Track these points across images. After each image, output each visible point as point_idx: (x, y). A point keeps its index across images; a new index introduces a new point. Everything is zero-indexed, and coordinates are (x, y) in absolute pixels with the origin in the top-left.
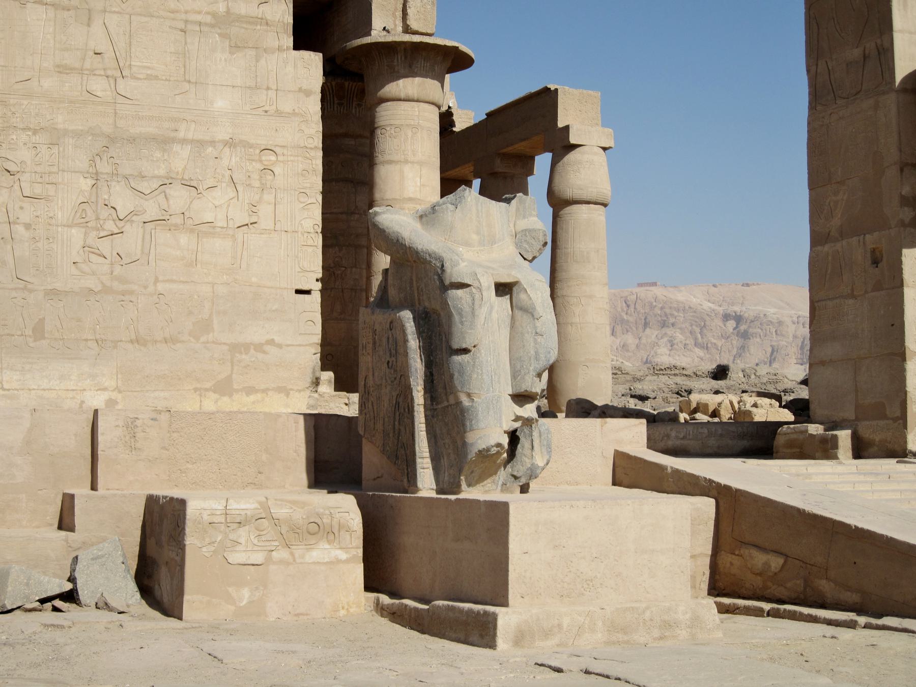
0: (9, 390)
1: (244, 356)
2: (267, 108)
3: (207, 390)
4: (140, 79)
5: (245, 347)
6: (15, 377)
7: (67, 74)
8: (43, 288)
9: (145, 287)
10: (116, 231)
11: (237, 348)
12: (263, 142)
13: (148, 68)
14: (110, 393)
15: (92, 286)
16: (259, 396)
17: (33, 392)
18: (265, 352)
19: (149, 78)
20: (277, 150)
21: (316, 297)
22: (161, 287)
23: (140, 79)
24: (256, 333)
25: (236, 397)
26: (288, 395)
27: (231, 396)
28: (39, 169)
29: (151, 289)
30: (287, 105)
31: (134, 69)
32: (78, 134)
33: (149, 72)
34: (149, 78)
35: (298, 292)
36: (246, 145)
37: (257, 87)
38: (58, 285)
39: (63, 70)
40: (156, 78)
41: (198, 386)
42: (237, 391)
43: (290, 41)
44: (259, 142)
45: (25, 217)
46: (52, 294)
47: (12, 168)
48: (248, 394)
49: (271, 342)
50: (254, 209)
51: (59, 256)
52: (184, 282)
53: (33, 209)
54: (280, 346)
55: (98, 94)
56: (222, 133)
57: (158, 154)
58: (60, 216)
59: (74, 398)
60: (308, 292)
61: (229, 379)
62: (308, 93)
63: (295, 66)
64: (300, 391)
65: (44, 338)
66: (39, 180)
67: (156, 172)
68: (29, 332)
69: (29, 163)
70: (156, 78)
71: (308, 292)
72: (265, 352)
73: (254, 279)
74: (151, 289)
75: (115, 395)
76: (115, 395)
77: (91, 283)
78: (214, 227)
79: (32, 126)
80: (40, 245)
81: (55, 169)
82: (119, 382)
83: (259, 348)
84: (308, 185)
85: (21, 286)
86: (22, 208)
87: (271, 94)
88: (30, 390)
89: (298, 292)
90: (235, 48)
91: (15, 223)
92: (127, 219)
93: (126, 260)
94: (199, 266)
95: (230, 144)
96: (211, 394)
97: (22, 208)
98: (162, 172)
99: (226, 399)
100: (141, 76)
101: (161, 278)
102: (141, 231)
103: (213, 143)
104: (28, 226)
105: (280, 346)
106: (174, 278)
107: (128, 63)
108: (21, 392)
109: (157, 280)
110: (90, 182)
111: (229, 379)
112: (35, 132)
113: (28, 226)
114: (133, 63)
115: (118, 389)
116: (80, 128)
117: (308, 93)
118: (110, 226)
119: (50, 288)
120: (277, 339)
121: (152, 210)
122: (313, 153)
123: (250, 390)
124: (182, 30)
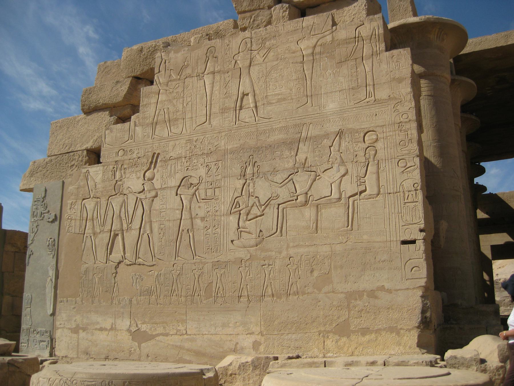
0: (190, 335)
1: (358, 302)
2: (367, 100)
3: (328, 332)
4: (274, 103)
5: (359, 294)
6: (194, 326)
7: (226, 112)
8: (212, 261)
9: (280, 253)
10: (259, 214)
11: (352, 296)
12: (366, 126)
13: (279, 94)
14: (257, 337)
15: (243, 256)
16: (373, 336)
17: (205, 336)
18: (376, 297)
19: (279, 101)
20: (378, 129)
21: (420, 245)
22: (292, 252)
23: (274, 103)
24: (366, 283)
25: (353, 337)
26: (398, 333)
27: (348, 337)
28: (210, 179)
29: (284, 253)
30: (382, 94)
31: (270, 98)
32: (232, 152)
33: (279, 97)
34: (279, 101)
35: (404, 242)
36: (352, 132)
37: (358, 87)
38: (222, 258)
39: (224, 110)
40: (284, 99)
41: (322, 329)
42: (354, 332)
43: (383, 46)
44: (363, 127)
45: (202, 214)
46: (217, 265)
47: (195, 181)
48: (363, 334)
49: (382, 288)
50: (362, 180)
51: (222, 237)
52: (308, 246)
53: (206, 207)
54: (389, 291)
55: (247, 120)
56: (334, 128)
57: (287, 153)
58: (222, 209)
59: (231, 341)
60: (413, 242)
61: (347, 321)
62: (400, 80)
63: (388, 63)
64: (409, 330)
65: (211, 296)
66: (210, 187)
67: (286, 166)
68: (202, 293)
69: (204, 176)
70: (284, 99)
71: (413, 242)
72: (376, 297)
73: (365, 237)
74: (284, 253)
75: (258, 338)
76: (258, 338)
77: (242, 254)
78: (330, 199)
79: (206, 152)
80: (210, 230)
81: (219, 177)
82: (262, 327)
83: (372, 294)
84: (406, 152)
85: (199, 261)
86: (199, 207)
87: (370, 88)
88: (203, 334)
89: (404, 242)
90: (340, 63)
91: (195, 218)
92: (267, 204)
93: (265, 233)
94: (319, 232)
95: (340, 133)
96: (331, 335)
97: (199, 207)
98: (291, 165)
99: (344, 339)
100: (274, 101)
101: (291, 244)
102: (276, 211)
103: (326, 136)
104: (203, 219)
105: (389, 291)
106: (301, 243)
107: (265, 95)
108: (198, 336)
109: (288, 247)
110: (242, 182)
111: (347, 321)
112: (208, 155)
113: (203, 219)
114: (269, 94)
115: (261, 333)
116: (236, 146)
117: (400, 80)
118: (255, 211)
119: (216, 260)
120: (387, 286)
121: (284, 194)
122: (408, 126)
123: (365, 331)
124: (301, 63)
